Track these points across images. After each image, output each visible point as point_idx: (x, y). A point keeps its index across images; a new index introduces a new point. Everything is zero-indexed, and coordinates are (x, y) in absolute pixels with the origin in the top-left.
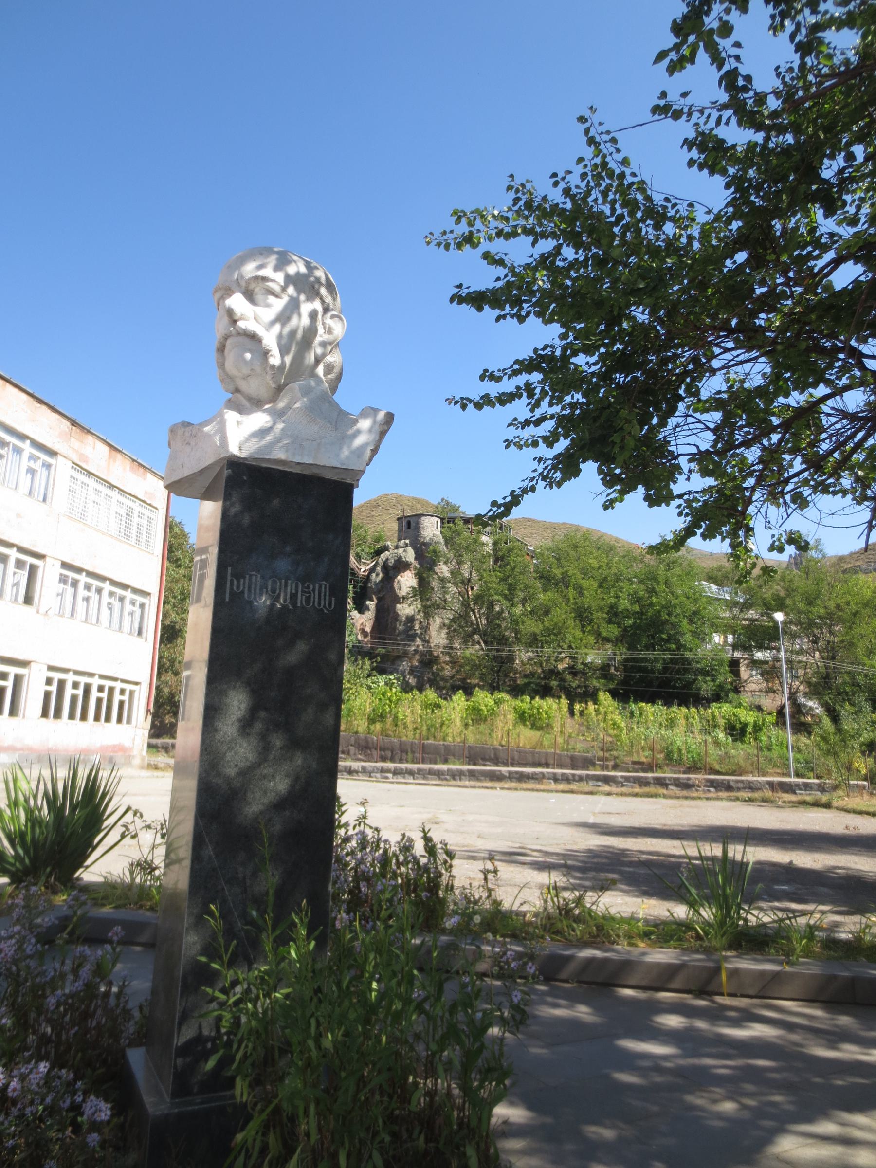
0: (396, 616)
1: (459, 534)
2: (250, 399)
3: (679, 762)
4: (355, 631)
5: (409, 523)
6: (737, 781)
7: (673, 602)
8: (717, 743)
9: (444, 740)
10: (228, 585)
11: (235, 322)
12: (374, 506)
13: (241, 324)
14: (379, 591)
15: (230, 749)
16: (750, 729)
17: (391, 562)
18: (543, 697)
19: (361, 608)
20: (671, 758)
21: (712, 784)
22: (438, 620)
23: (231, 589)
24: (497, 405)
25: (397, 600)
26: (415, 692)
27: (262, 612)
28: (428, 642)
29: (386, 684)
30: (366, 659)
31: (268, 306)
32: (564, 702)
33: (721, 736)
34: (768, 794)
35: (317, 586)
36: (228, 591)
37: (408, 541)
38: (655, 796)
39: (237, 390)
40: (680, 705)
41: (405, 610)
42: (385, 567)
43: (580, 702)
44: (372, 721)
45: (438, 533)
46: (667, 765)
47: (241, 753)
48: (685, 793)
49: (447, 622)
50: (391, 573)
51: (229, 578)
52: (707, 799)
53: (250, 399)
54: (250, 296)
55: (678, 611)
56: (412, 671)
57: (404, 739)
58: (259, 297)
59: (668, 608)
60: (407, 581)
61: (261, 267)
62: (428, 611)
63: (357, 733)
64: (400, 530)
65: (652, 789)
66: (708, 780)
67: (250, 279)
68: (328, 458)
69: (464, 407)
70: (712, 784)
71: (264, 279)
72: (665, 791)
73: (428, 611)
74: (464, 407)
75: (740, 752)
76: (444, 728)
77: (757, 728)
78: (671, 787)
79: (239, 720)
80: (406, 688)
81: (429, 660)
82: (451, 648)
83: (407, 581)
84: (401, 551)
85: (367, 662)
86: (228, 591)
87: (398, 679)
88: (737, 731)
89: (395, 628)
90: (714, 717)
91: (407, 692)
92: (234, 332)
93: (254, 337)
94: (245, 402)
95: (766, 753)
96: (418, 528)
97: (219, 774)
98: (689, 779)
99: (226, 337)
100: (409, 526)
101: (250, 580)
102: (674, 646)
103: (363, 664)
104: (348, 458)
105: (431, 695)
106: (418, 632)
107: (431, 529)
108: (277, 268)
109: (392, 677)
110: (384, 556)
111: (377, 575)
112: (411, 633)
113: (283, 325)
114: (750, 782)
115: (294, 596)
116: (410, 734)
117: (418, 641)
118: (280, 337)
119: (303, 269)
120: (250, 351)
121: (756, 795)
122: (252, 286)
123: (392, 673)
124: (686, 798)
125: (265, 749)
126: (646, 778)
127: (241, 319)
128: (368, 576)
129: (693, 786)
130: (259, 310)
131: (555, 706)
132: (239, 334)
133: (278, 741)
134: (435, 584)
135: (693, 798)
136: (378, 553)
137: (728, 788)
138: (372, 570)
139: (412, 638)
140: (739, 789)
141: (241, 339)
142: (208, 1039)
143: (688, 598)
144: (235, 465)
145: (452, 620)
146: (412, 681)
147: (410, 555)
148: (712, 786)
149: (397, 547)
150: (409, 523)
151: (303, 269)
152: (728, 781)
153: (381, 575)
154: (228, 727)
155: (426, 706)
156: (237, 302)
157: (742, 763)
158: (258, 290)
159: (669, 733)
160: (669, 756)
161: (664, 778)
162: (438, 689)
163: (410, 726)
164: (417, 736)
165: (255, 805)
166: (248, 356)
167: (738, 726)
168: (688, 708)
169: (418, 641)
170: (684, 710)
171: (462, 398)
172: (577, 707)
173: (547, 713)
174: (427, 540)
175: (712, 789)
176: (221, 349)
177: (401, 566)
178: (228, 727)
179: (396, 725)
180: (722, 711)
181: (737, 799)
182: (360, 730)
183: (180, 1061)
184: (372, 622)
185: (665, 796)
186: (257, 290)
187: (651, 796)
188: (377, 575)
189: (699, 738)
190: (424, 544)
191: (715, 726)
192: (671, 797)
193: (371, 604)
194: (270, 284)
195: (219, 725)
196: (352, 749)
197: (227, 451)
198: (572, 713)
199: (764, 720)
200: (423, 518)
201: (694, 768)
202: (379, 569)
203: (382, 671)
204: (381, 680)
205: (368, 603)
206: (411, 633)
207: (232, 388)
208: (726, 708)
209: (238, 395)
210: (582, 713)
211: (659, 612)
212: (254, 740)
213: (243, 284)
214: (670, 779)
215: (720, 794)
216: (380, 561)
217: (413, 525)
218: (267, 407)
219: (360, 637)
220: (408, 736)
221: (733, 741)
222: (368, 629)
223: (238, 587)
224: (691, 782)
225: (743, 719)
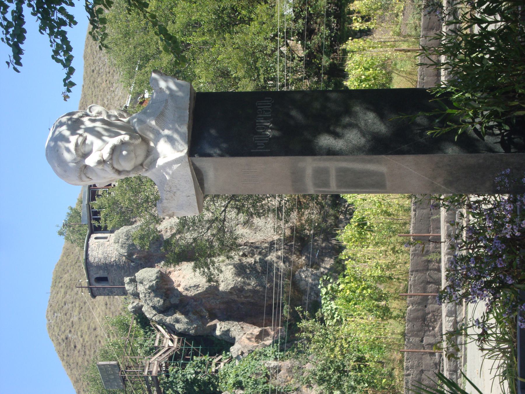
0: (237, 290)
1: (115, 203)
2: (147, 156)
4: (260, 349)
5: (100, 280)
9: (408, 210)
10: (261, 150)
12: (68, 345)
13: (106, 156)
14: (202, 317)
15: (351, 142)
17: (158, 301)
18: (345, 76)
19: (226, 343)
22: (240, 230)
23: (263, 149)
24: (71, 53)
25: (212, 291)
26: (343, 256)
27: (276, 133)
28: (272, 243)
29: (333, 298)
30: (299, 325)
31: (92, 143)
32: (350, 44)
35: (259, 107)
36: (264, 150)
37: (127, 279)
39: (142, 165)
41: (227, 278)
42: (165, 310)
43: (351, 22)
44: (385, 313)
45: (112, 237)
47: (353, 137)
49: (242, 217)
50: (174, 301)
51: (257, 150)
53: (147, 156)
54: (86, 155)
56: (314, 264)
57: (409, 266)
58: (87, 149)
60: (186, 278)
61: (68, 150)
62: (228, 245)
63: (403, 334)
64: (110, 293)
68: (186, 103)
69: (72, 84)
71: (77, 145)
73: (228, 245)
74: (72, 84)
76: (390, 210)
79: (335, 139)
80: (338, 270)
81: (298, 241)
82: (280, 209)
83: (186, 278)
84: (141, 289)
85: (304, 324)
86: (264, 150)
87: (326, 283)
89: (254, 291)
91: (344, 268)
92: (111, 162)
93: (114, 149)
94: (149, 159)
96: (107, 267)
97: (364, 146)
99: (113, 168)
100: (103, 279)
101: (257, 140)
103: (306, 330)
104: (183, 92)
105: (347, 234)
106: (258, 257)
107: (107, 247)
108: (68, 141)
109: (324, 291)
110: (149, 313)
111: (177, 321)
112: (259, 268)
113: (103, 135)
115: (266, 119)
116: (402, 258)
117: (272, 257)
118: (110, 137)
119: (64, 128)
122: (81, 154)
123: (320, 292)
125: (350, 126)
127: (103, 158)
128: (180, 334)
130: (95, 148)
131: (357, 57)
132: (111, 159)
133: (347, 120)
134: (189, 237)
136: (144, 322)
138: (170, 329)
139: (267, 267)
141: (115, 157)
142: (502, 139)
144: (191, 153)
145: (239, 210)
146: (328, 263)
147: (148, 275)
149: (136, 295)
150: (100, 280)
151: (64, 128)
153: (178, 315)
154: (338, 144)
155: (361, 240)
156: (91, 161)
158: (82, 150)
162: (337, 224)
163: (392, 257)
164: (403, 248)
165: (381, 128)
166: (124, 153)
169: (272, 257)
171: (65, 85)
172: (357, 26)
173: (367, 69)
174: (124, 251)
177: (163, 287)
178: (338, 144)
179: (390, 278)
182: (399, 329)
183: (512, 150)
184: (246, 326)
186: (82, 151)
188: (177, 321)
190: (129, 256)
193: (220, 327)
194: (79, 142)
195: (338, 148)
196: (427, 340)
197: (184, 156)
198: (365, 33)
200: (91, 259)
202: (168, 319)
203: (316, 305)
204: (328, 306)
205: (218, 333)
206: (259, 268)
207: (140, 167)
209: (145, 163)
210: (366, 19)
212: (346, 131)
213: (79, 159)
216: (157, 318)
217: (101, 274)
218: (152, 144)
219: (269, 341)
220: (405, 260)
222: (256, 330)
223: (262, 146)
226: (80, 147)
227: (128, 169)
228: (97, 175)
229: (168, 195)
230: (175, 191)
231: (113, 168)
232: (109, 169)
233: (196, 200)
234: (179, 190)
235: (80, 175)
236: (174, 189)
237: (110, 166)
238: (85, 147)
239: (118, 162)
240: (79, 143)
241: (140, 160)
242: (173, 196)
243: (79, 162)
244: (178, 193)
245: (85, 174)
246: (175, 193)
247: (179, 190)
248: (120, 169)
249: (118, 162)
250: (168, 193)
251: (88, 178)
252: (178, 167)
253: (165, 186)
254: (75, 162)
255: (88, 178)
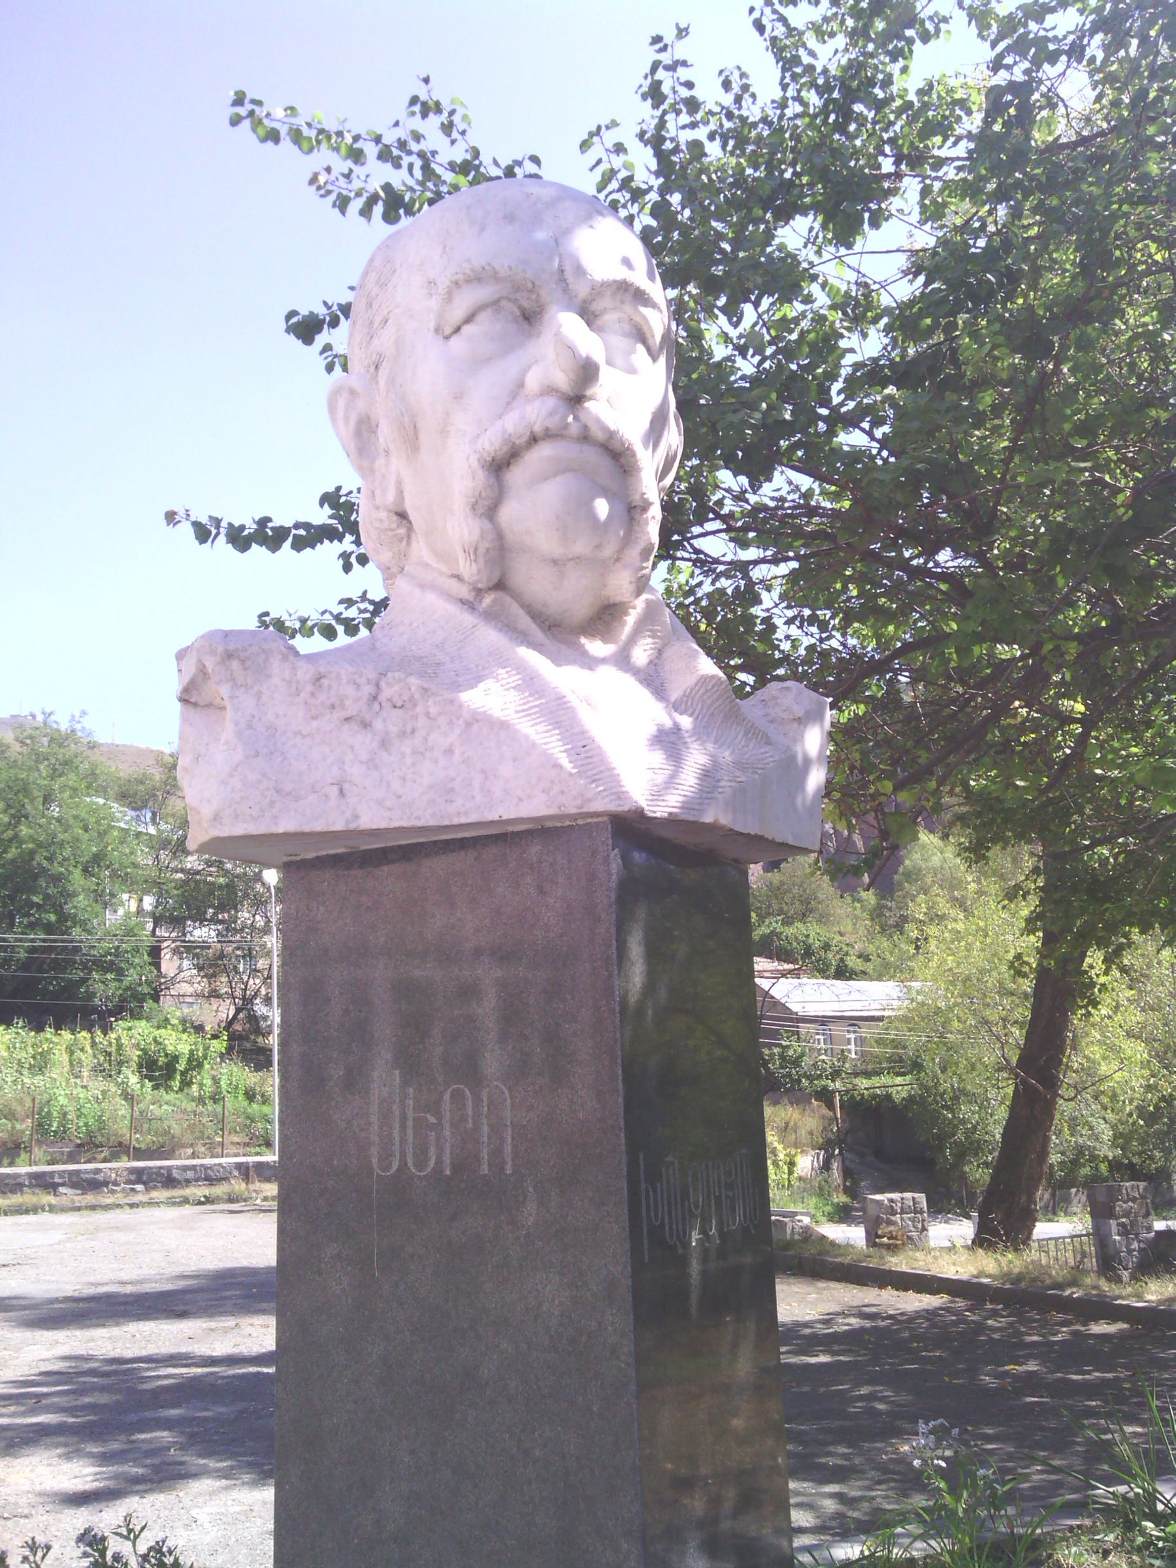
3: (62, 1135)
6: (185, 1168)
7: (61, 836)
8: (128, 1097)
11: (576, 400)
16: (181, 1066)
20: (46, 1129)
21: (139, 1176)
23: (649, 1219)
31: (632, 370)
33: (134, 1080)
34: (239, 1186)
38: (34, 1210)
39: (500, 585)
40: (58, 1027)
46: (39, 1143)
48: (90, 1198)
51: (643, 1186)
52: (132, 1206)
55: (67, 852)
59: (51, 845)
65: (26, 1198)
66: (132, 1171)
67: (605, 285)
70: (139, 1176)
72: (52, 1199)
75: (167, 1107)
77: (195, 1063)
78: (62, 1190)
88: (159, 1069)
90: (120, 1047)
92: (574, 429)
94: (526, 622)
95: (210, 1106)
98: (98, 1171)
102: (53, 918)
114: (206, 1168)
120: (606, 493)
121: (219, 1190)
124: (93, 1208)
126: (16, 1176)
129: (106, 1183)
132: (585, 437)
135: (107, 1208)
137: (169, 1181)
140: (188, 1182)
141: (592, 455)
143: (86, 830)
148: (138, 1181)
152: (169, 1169)
157: (176, 1130)
159: (38, 1080)
160: (41, 1127)
161: (52, 1173)
166: (602, 507)
167: (162, 1060)
168: (73, 1032)
170: (66, 1035)
175: (139, 1187)
176: (499, 466)
180: (132, 1034)
181: (185, 1201)
185: (52, 1209)
187: (27, 1212)
189: (98, 1086)
191: (120, 1063)
192: (63, 1210)
194: (646, 311)
197: (621, 795)
199: (206, 1048)
201: (88, 1146)
208: (142, 1028)
209: (508, 600)
211: (32, 853)
213: (583, 291)
214: (61, 1174)
215: (154, 1194)
221: (156, 1087)
224: (100, 1177)
225: (170, 1049)
226: (628, 308)
227: (508, 512)
228: (479, 362)
229: (350, 691)
230: (378, 725)
231: (534, 440)
232: (536, 413)
233: (318, 827)
234: (384, 744)
235: (496, 277)
236: (390, 722)
237: (552, 423)
238: (625, 335)
239: (561, 468)
240: (643, 310)
241: (536, 582)
242: (338, 715)
243: (566, 290)
244: (363, 742)
245: (495, 304)
246: (366, 725)
247: (384, 744)
248: (517, 475)
249: (561, 468)
250: (368, 689)
251: (469, 319)
252: (547, 756)
253: (414, 681)
254: (568, 269)
255: (469, 319)
